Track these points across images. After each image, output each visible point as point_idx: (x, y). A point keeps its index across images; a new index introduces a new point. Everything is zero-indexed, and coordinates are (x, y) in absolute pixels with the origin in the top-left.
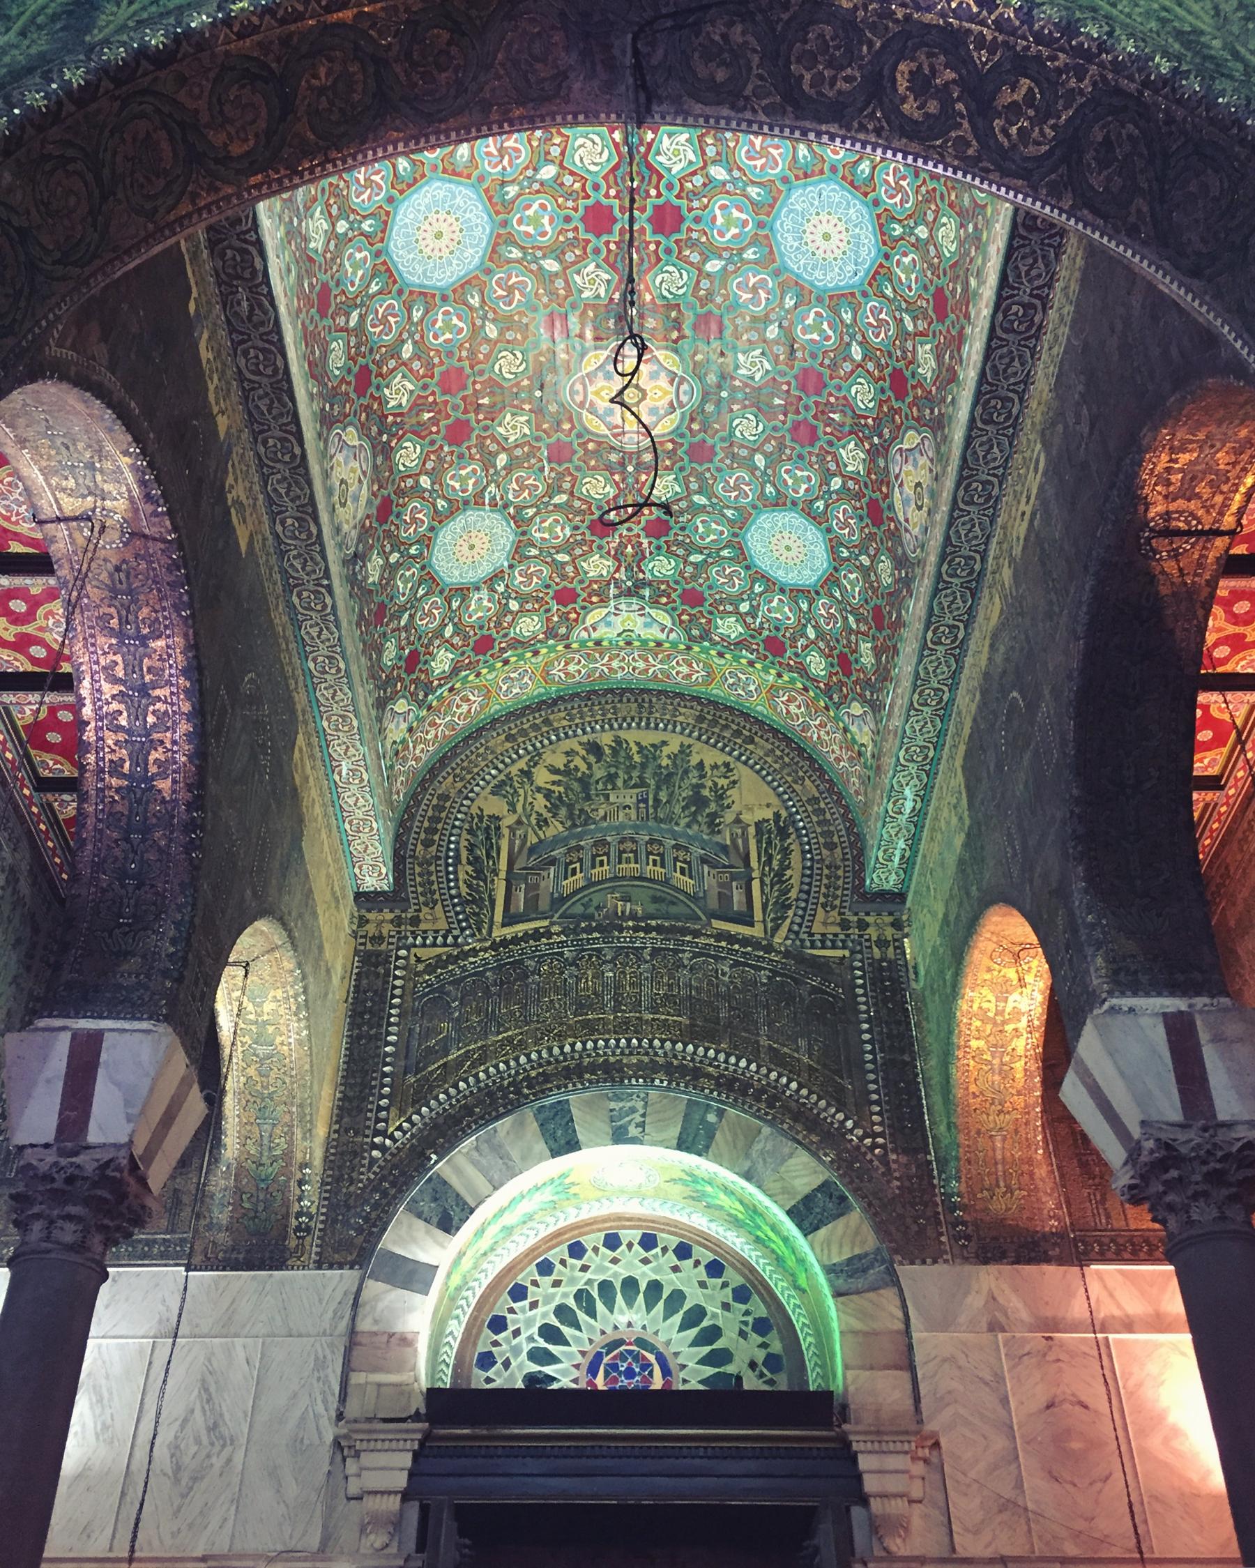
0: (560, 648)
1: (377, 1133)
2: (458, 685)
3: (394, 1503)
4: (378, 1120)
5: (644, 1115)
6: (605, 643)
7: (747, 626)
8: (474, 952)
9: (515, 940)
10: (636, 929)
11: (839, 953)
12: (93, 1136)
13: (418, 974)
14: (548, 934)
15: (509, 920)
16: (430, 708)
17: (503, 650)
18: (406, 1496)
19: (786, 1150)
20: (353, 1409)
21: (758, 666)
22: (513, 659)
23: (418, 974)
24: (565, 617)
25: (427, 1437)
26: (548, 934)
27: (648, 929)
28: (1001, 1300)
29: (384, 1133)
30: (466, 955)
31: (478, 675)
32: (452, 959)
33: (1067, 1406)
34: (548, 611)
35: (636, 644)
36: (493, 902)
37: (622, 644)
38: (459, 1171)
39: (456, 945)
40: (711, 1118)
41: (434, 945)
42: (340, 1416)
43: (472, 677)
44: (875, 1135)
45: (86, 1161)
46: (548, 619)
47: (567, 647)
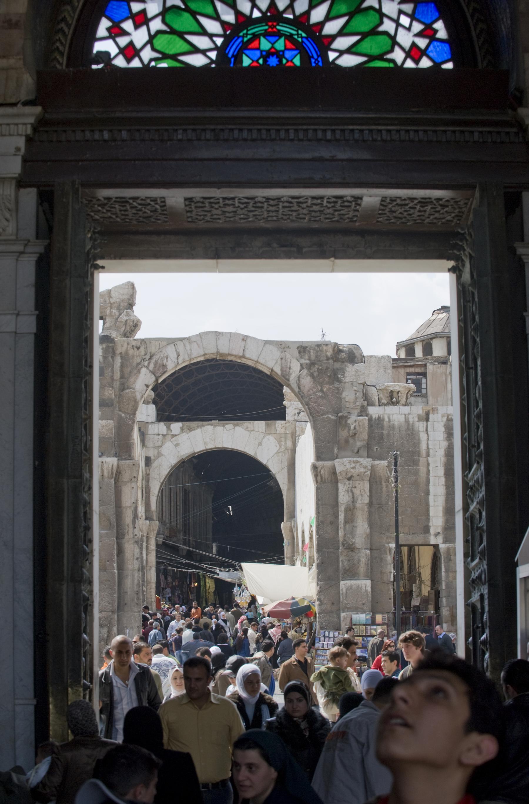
18: (21, 183)
25: (41, 124)
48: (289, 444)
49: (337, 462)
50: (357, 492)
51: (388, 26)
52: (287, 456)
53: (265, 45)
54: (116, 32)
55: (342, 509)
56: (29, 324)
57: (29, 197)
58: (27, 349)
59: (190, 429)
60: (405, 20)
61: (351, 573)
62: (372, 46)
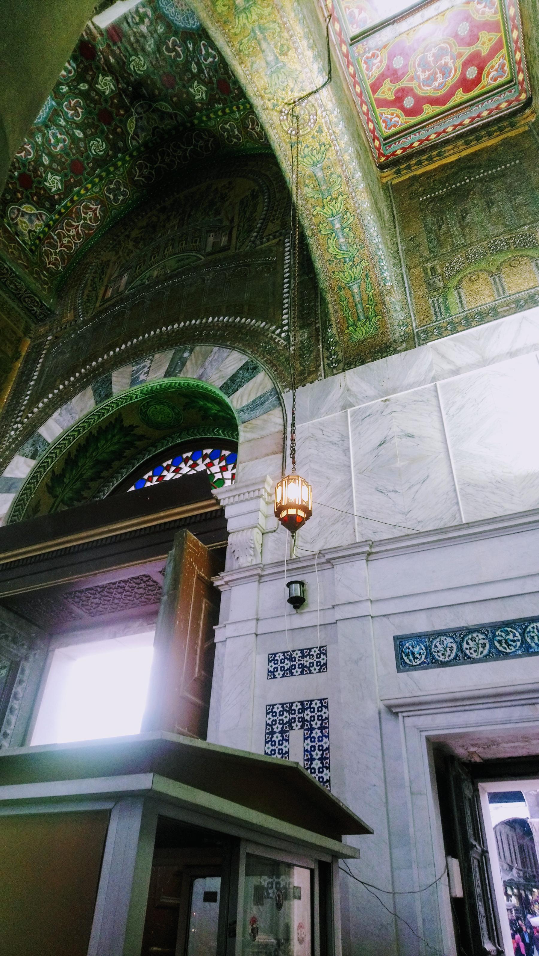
0: (127, 158)
2: (76, 198)
5: (149, 367)
6: (150, 145)
7: (204, 83)
16: (60, 214)
17: (93, 169)
19: (225, 355)
21: (227, 110)
22: (104, 174)
24: (114, 132)
28: (354, 389)
31: (86, 189)
33: (396, 440)
34: (102, 132)
35: (166, 136)
37: (158, 141)
43: (83, 192)
46: (107, 138)
47: (131, 155)
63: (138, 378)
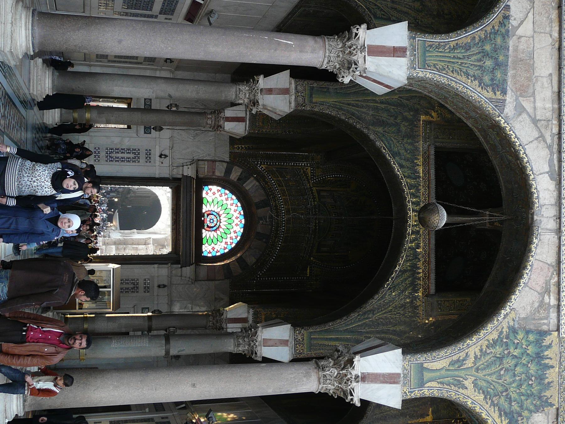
1: (261, 162)
3: (181, 173)
4: (264, 163)
8: (309, 183)
9: (312, 193)
10: (316, 223)
11: (308, 274)
12: (226, 123)
13: (303, 169)
14: (314, 201)
15: (319, 192)
18: (183, 175)
20: (200, 163)
23: (303, 169)
25: (194, 179)
26: (314, 201)
27: (315, 226)
29: (261, 164)
30: (308, 180)
32: (307, 177)
36: (324, 187)
38: (251, 182)
39: (311, 178)
40: (264, 240)
41: (311, 173)
42: (199, 160)
44: (260, 278)
45: (221, 123)
48: (162, 233)
49: (152, 245)
50: (142, 251)
51: (219, 243)
52: (159, 232)
53: (215, 220)
54: (219, 191)
55: (137, 246)
56: (157, 176)
57: (180, 176)
58: (152, 176)
59: (168, 199)
60: (220, 247)
61: (117, 249)
62: (215, 240)
63: (262, 220)
